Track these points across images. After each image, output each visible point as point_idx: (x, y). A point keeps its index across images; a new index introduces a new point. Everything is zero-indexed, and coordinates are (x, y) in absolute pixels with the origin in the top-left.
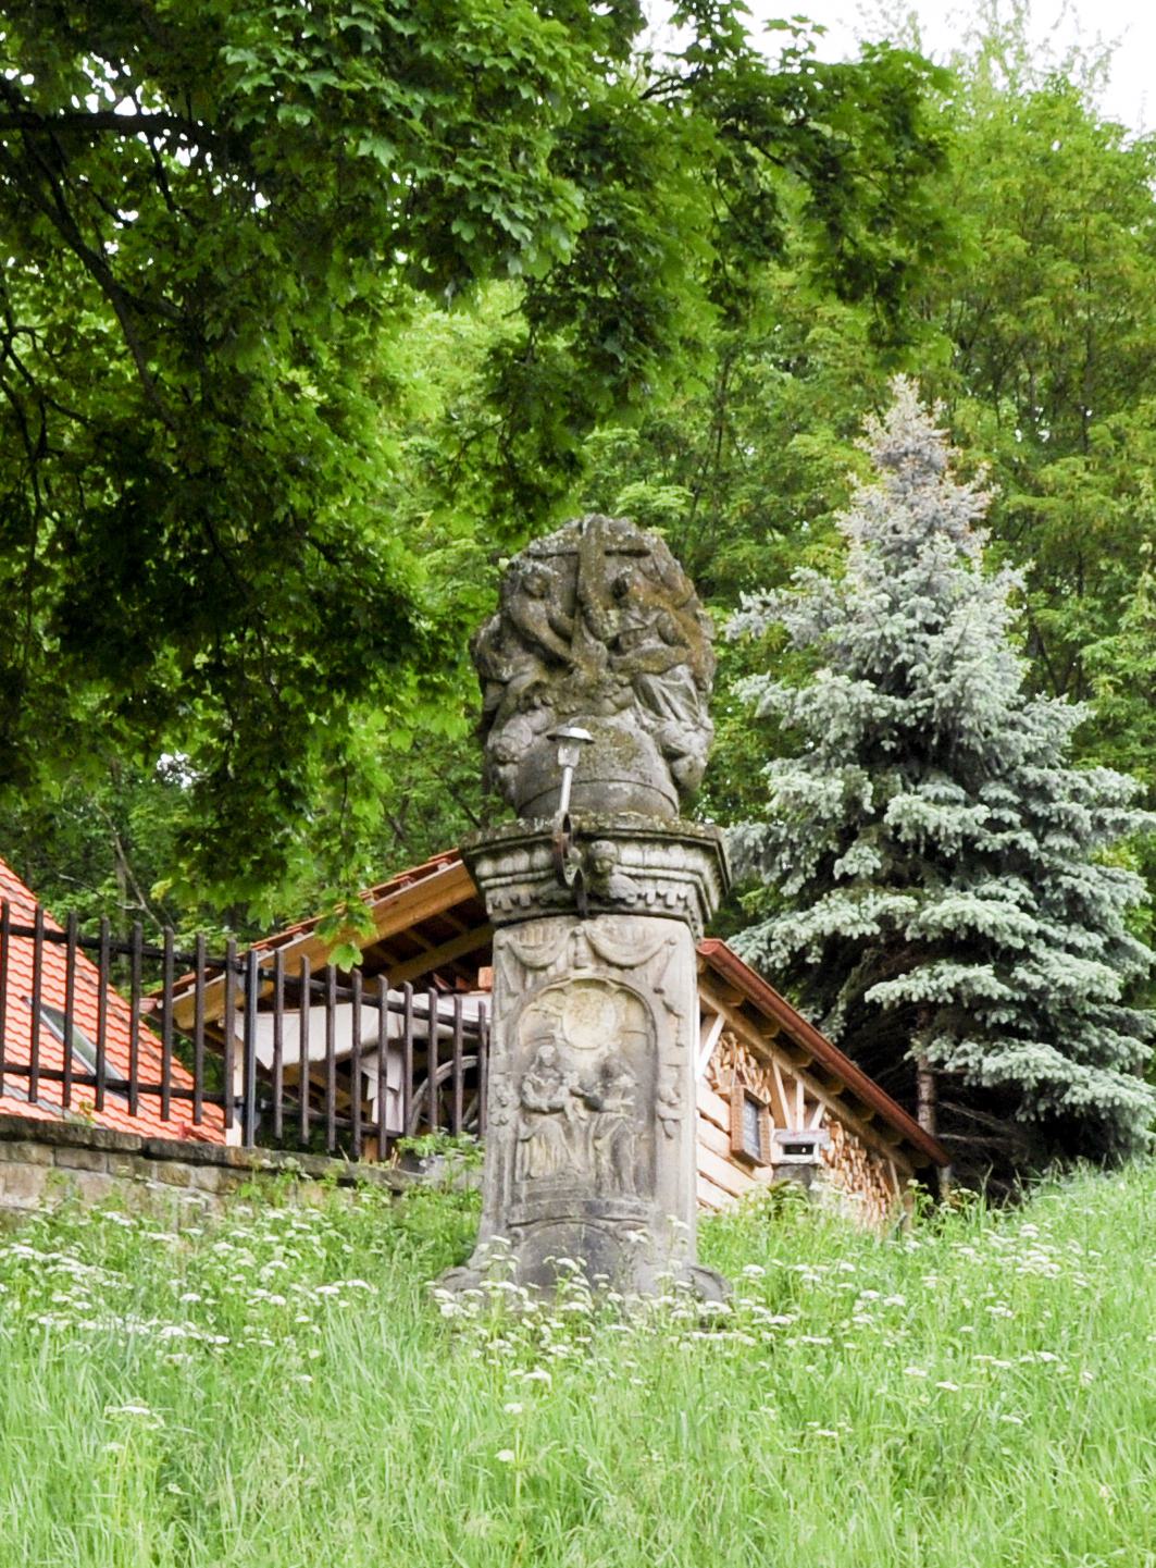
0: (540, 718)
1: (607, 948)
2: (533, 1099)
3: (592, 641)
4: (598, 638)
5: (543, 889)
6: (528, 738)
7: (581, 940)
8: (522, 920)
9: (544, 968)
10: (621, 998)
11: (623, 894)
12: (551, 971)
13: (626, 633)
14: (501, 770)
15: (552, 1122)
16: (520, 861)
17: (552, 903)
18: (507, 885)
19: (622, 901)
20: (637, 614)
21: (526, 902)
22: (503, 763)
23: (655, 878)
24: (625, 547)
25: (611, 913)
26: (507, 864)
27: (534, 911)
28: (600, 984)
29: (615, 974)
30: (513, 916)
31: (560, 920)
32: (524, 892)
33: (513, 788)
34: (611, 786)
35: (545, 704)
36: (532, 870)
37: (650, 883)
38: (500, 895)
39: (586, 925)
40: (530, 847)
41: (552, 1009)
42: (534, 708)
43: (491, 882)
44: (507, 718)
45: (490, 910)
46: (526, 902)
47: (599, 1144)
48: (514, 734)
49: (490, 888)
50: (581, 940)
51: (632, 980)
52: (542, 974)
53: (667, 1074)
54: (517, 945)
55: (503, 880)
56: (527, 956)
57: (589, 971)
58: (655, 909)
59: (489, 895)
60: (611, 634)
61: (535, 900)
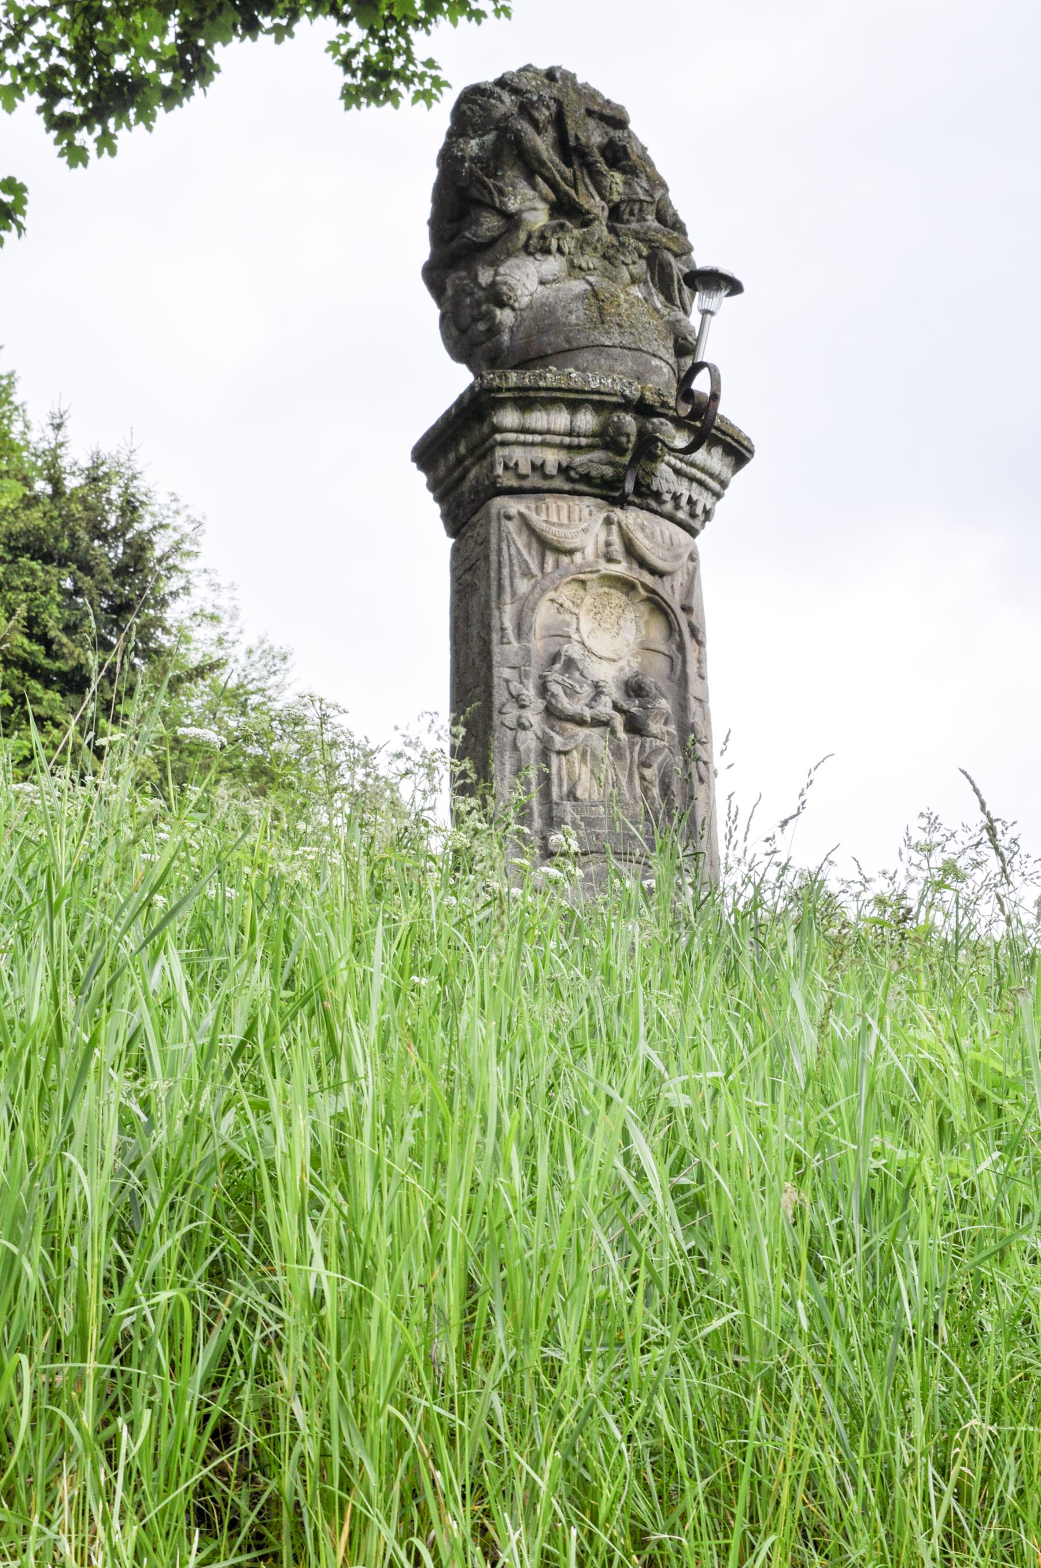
0: (553, 265)
1: (643, 543)
2: (566, 704)
3: (598, 199)
4: (603, 198)
5: (579, 459)
6: (532, 285)
7: (615, 528)
8: (535, 491)
9: (570, 552)
10: (644, 608)
11: (664, 487)
12: (578, 557)
13: (631, 201)
14: (498, 312)
15: (595, 737)
16: (560, 419)
17: (586, 479)
18: (533, 444)
19: (657, 495)
20: (645, 185)
21: (551, 469)
22: (502, 305)
23: (692, 479)
24: (608, 112)
25: (641, 507)
26: (538, 419)
27: (559, 483)
28: (627, 586)
29: (648, 579)
30: (527, 484)
31: (588, 501)
32: (552, 458)
33: (506, 337)
34: (655, 362)
35: (560, 250)
36: (570, 434)
37: (685, 483)
38: (522, 457)
39: (618, 514)
40: (574, 406)
41: (567, 604)
42: (547, 251)
43: (511, 437)
44: (509, 255)
45: (499, 470)
46: (551, 469)
47: (647, 772)
48: (517, 274)
49: (504, 444)
50: (615, 528)
51: (663, 588)
52: (565, 560)
53: (693, 705)
54: (538, 520)
55: (529, 438)
56: (553, 534)
57: (621, 569)
58: (681, 515)
59: (500, 453)
60: (616, 198)
61: (564, 471)
